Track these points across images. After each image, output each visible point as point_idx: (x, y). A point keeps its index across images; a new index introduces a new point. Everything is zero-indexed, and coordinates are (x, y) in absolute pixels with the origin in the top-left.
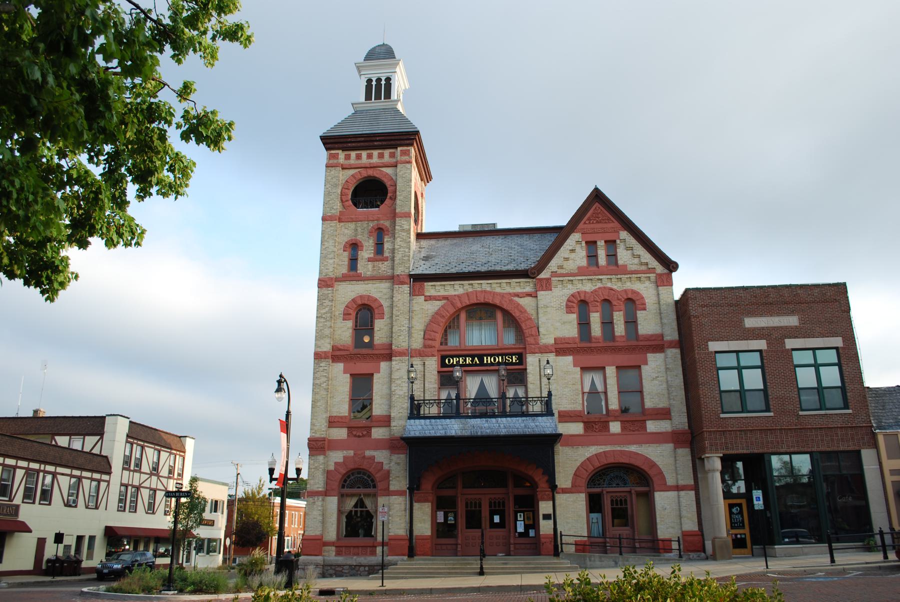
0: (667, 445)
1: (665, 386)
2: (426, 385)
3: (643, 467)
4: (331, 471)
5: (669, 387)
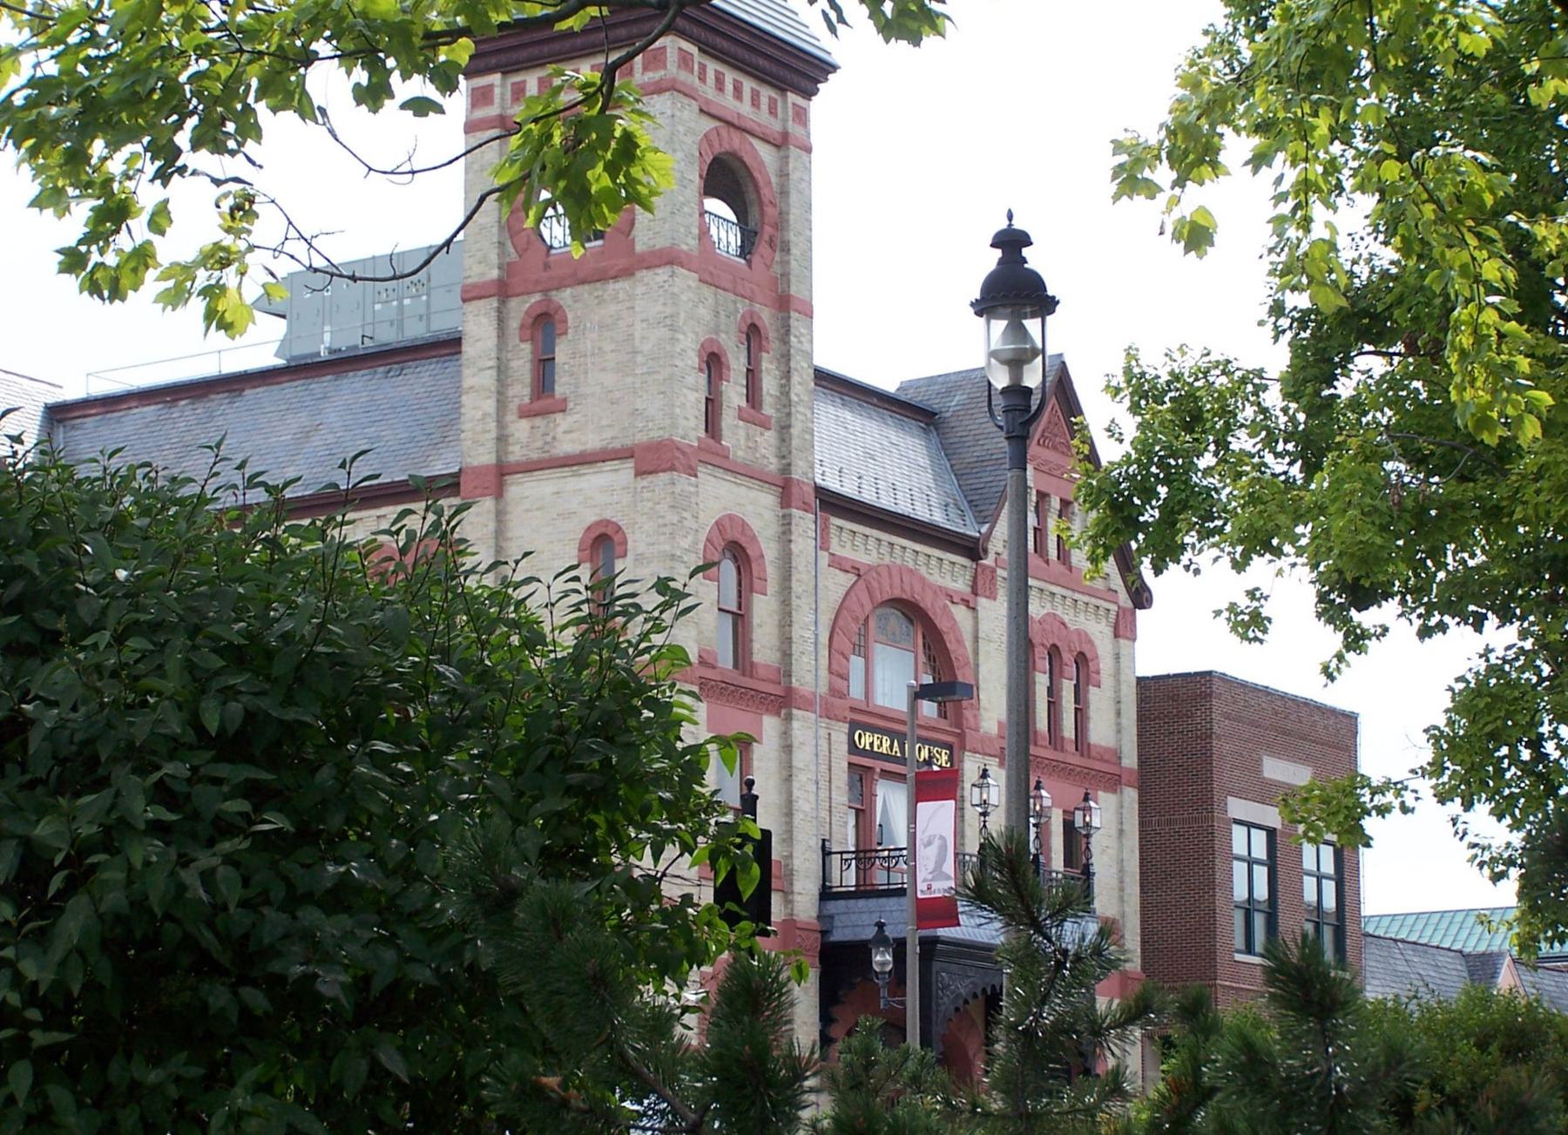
1: (1114, 870)
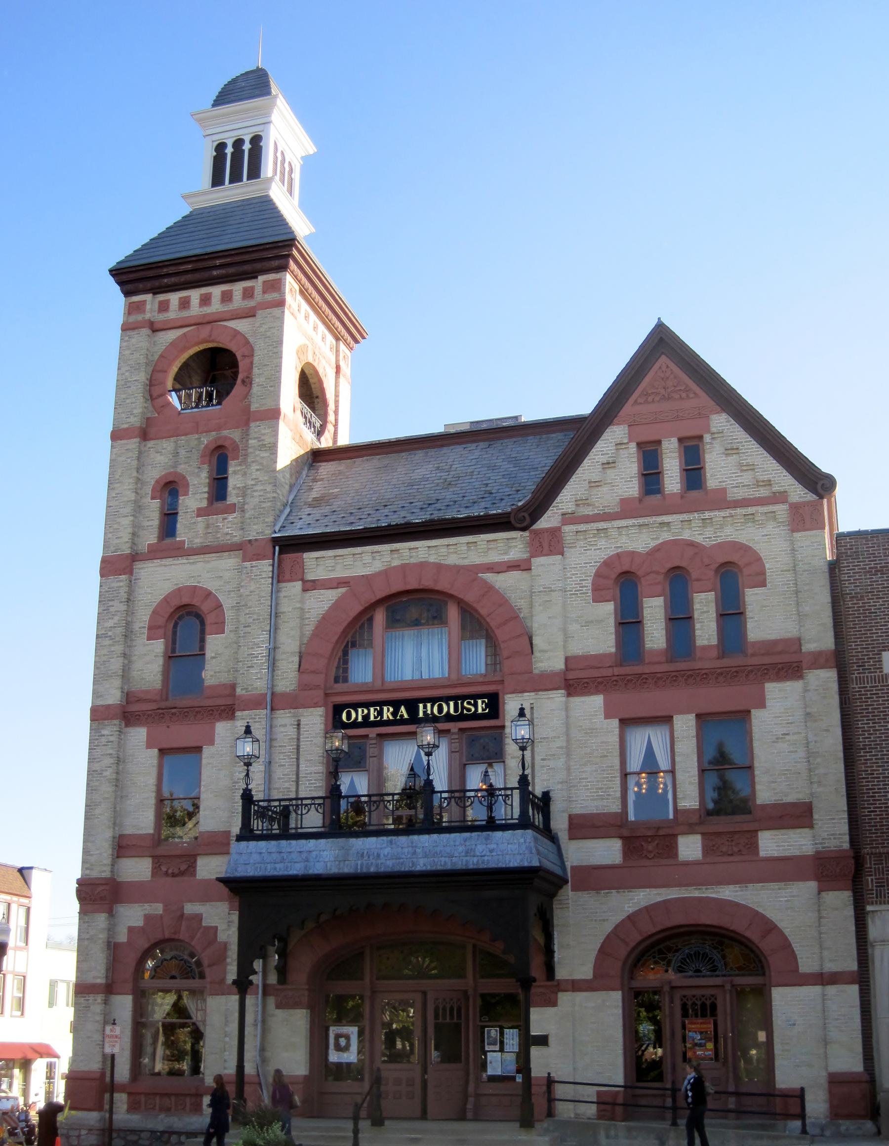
0: (801, 884)
1: (801, 753)
2: (303, 767)
3: (748, 934)
4: (123, 943)
5: (810, 755)
